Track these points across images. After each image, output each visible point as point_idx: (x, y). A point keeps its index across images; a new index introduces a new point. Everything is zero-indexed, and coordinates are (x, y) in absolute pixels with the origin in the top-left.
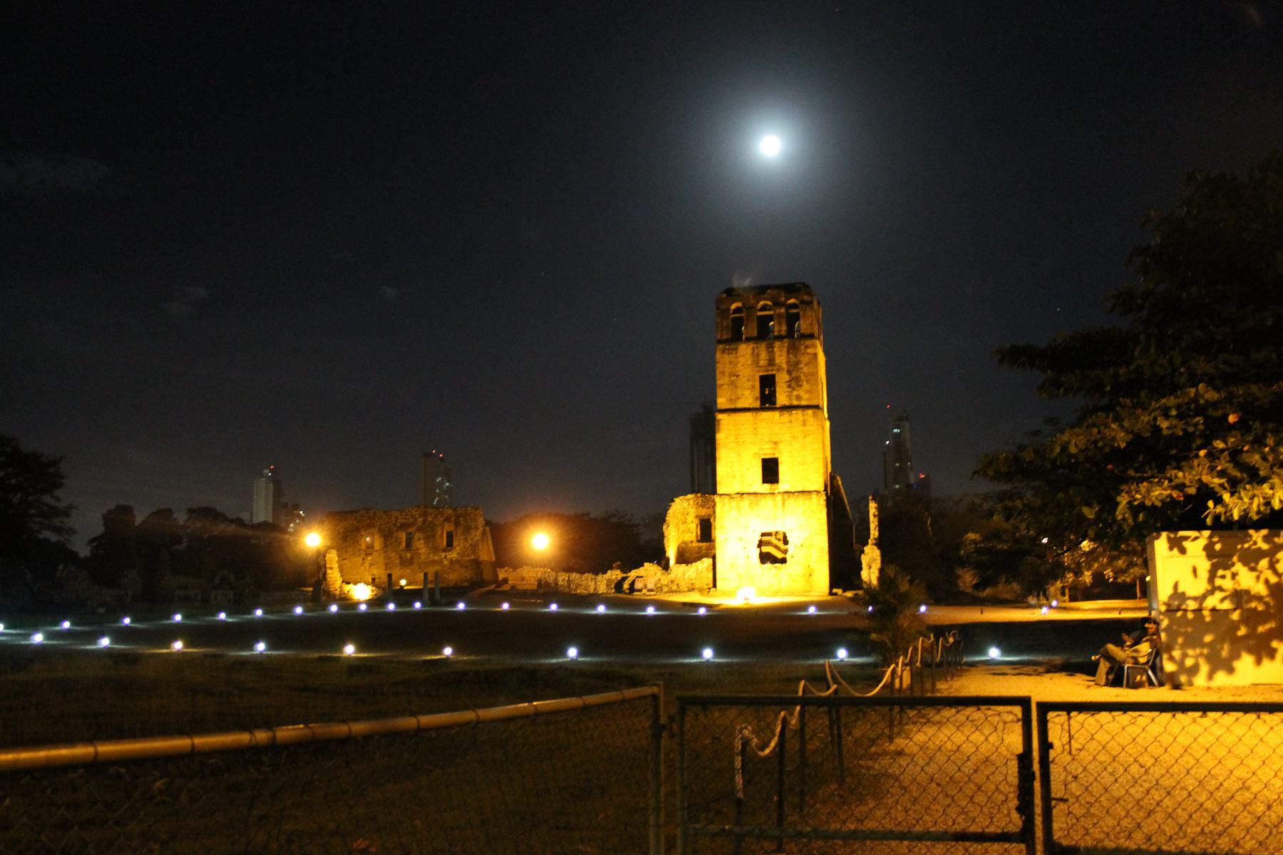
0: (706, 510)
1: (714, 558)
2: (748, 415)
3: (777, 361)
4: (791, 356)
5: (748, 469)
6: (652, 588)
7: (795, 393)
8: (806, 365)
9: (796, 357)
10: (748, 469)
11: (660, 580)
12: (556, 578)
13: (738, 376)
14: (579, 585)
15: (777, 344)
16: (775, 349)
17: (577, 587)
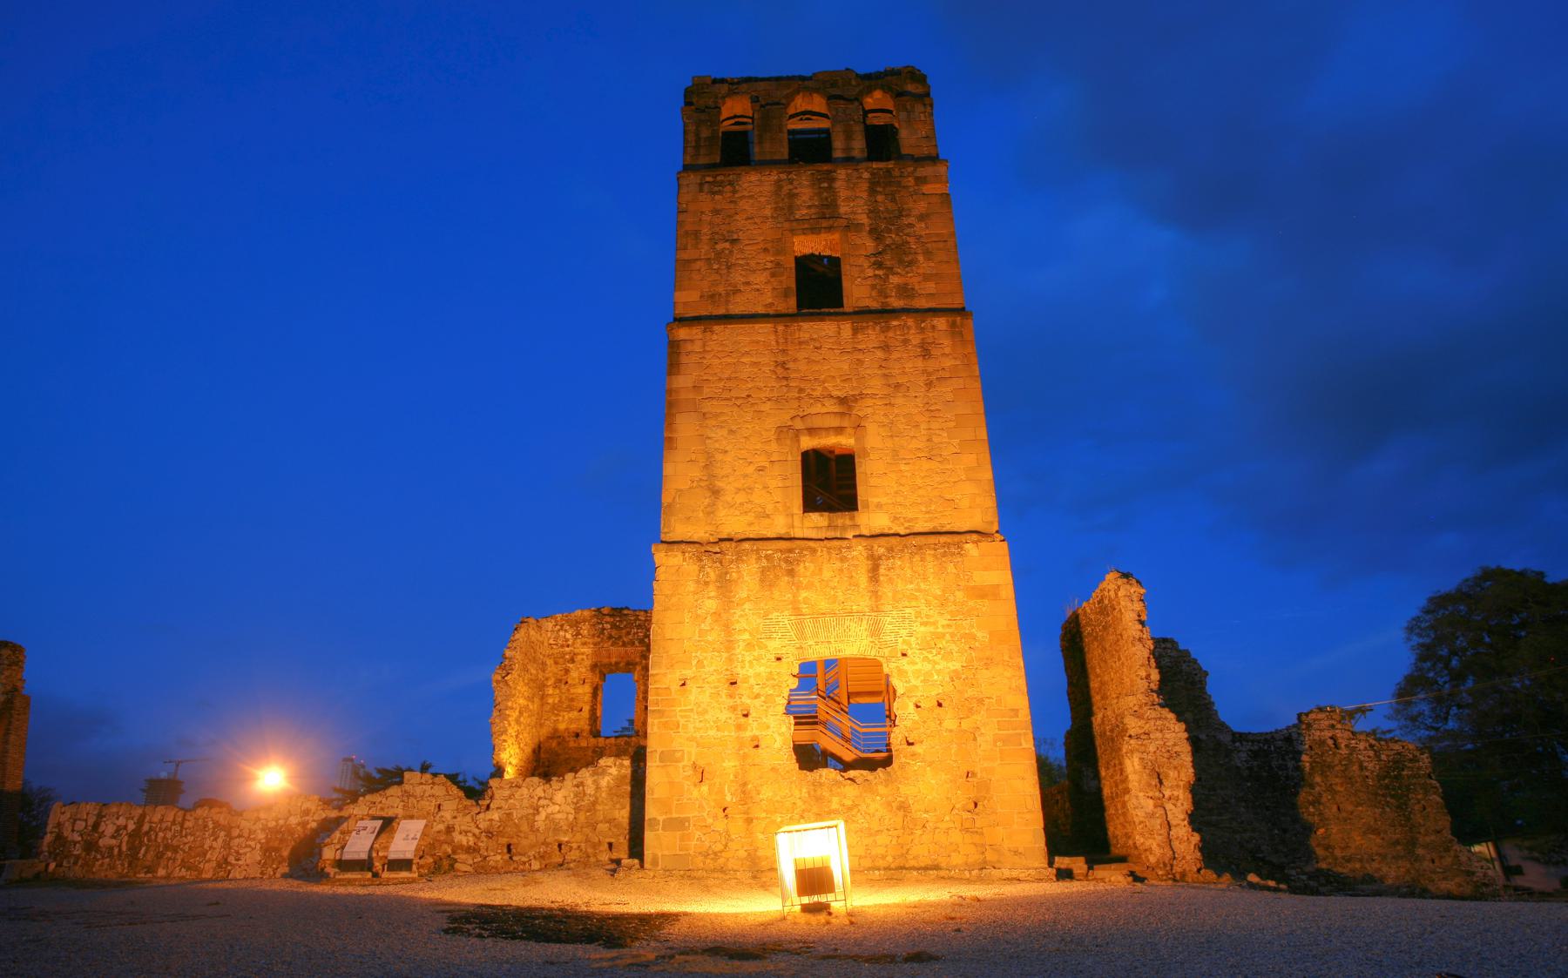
0: (622, 649)
1: (639, 758)
2: (763, 330)
3: (843, 209)
4: (880, 198)
5: (761, 469)
6: (409, 856)
7: (894, 280)
8: (922, 218)
9: (893, 200)
10: (761, 469)
11: (450, 830)
12: (96, 826)
13: (734, 241)
14: (167, 847)
15: (841, 173)
16: (838, 184)
17: (159, 856)
